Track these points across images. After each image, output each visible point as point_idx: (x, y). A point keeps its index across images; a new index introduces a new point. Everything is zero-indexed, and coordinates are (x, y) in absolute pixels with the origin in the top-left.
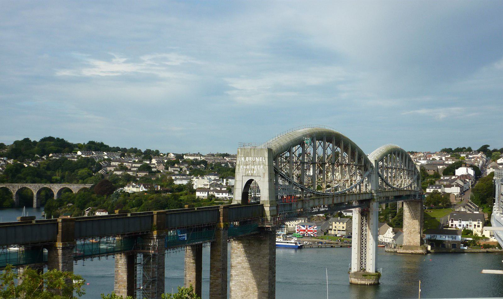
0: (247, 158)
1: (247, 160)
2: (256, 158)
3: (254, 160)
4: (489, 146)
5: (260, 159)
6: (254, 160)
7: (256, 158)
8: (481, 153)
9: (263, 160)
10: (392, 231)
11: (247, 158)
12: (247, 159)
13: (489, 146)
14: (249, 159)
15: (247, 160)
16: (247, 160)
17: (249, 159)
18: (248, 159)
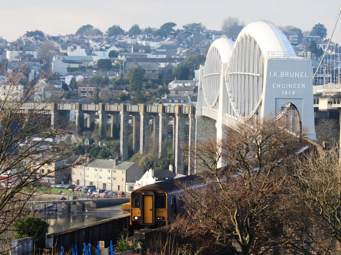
0: (281, 73)
1: (281, 76)
2: (296, 73)
3: (292, 75)
4: (174, 25)
5: (301, 75)
6: (292, 75)
7: (296, 73)
8: (169, 38)
9: (306, 77)
10: (153, 176)
11: (281, 73)
12: (281, 74)
13: (174, 25)
14: (285, 74)
15: (282, 75)
16: (282, 75)
17: (285, 74)
18: (283, 74)
